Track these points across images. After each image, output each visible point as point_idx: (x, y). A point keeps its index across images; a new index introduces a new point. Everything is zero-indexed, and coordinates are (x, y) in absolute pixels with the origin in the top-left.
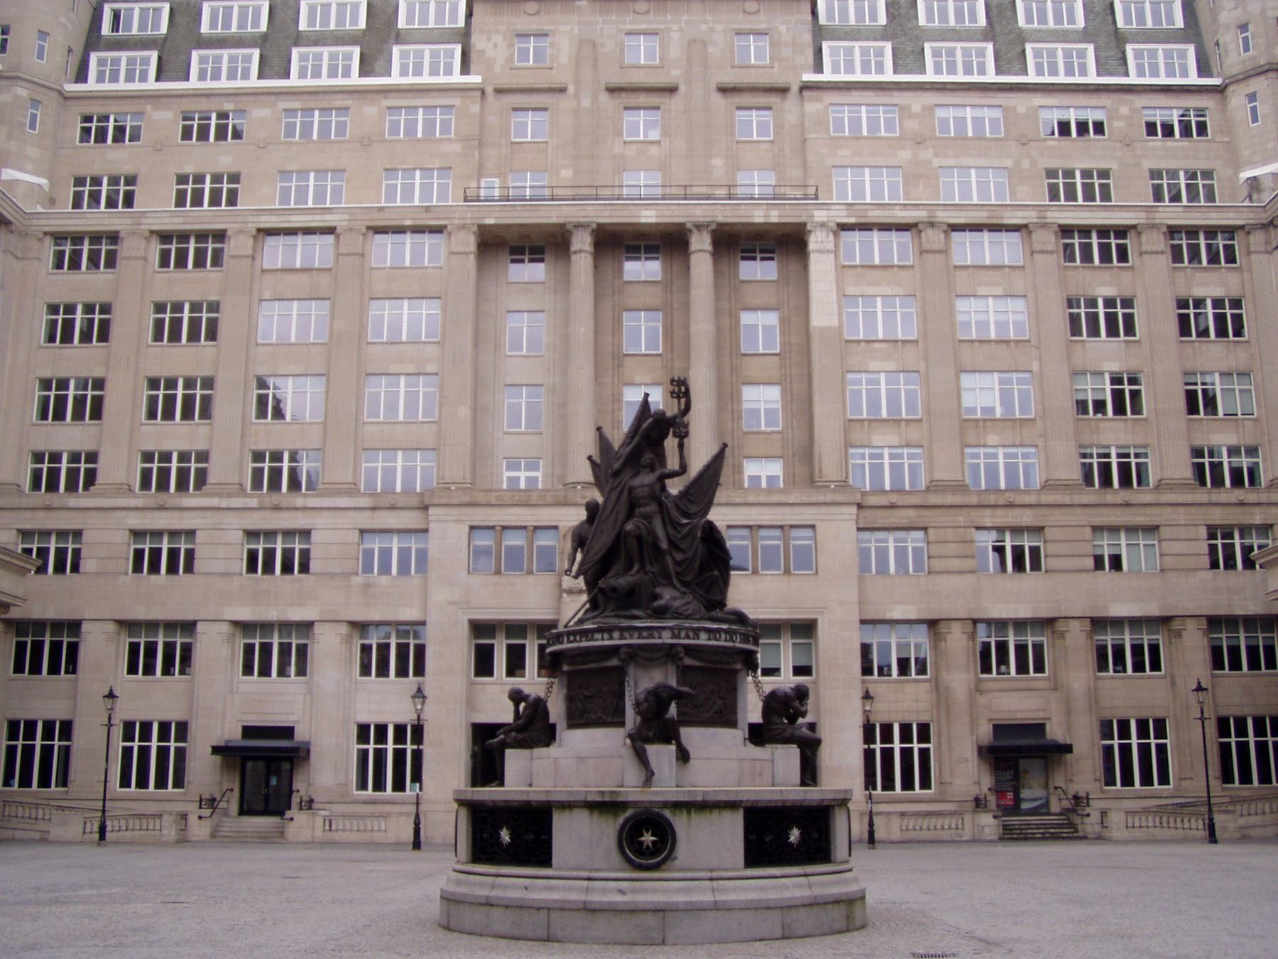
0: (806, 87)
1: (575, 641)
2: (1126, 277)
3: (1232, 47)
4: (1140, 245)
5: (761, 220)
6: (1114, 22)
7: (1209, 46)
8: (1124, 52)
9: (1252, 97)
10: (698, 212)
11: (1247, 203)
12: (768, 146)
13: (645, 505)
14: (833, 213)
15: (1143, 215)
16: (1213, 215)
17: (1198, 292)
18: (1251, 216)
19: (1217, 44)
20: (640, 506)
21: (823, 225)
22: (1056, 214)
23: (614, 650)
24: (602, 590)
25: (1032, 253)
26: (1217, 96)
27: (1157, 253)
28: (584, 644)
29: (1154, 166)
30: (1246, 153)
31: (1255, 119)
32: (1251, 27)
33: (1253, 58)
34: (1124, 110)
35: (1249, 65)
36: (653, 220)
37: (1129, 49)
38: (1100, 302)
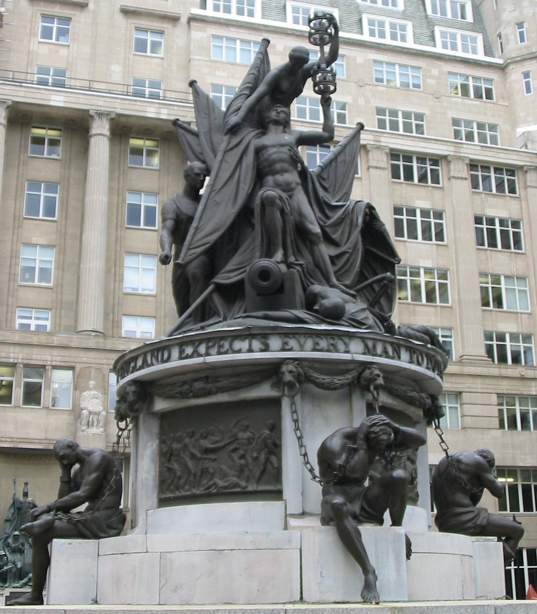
0: (192, 19)
2: (437, 194)
3: (511, 37)
4: (449, 171)
5: (153, 116)
6: (425, 10)
7: (493, 37)
8: (433, 32)
10: (100, 103)
11: (523, 150)
12: (159, 61)
13: (283, 171)
15: (452, 149)
16: (501, 155)
17: (490, 212)
18: (528, 159)
19: (500, 36)
22: (388, 140)
23: (271, 371)
24: (219, 288)
25: (368, 169)
27: (462, 178)
28: (215, 358)
29: (456, 116)
30: (522, 114)
32: (525, 25)
33: (527, 47)
34: (435, 72)
36: (61, 105)
37: (437, 30)
38: (418, 213)
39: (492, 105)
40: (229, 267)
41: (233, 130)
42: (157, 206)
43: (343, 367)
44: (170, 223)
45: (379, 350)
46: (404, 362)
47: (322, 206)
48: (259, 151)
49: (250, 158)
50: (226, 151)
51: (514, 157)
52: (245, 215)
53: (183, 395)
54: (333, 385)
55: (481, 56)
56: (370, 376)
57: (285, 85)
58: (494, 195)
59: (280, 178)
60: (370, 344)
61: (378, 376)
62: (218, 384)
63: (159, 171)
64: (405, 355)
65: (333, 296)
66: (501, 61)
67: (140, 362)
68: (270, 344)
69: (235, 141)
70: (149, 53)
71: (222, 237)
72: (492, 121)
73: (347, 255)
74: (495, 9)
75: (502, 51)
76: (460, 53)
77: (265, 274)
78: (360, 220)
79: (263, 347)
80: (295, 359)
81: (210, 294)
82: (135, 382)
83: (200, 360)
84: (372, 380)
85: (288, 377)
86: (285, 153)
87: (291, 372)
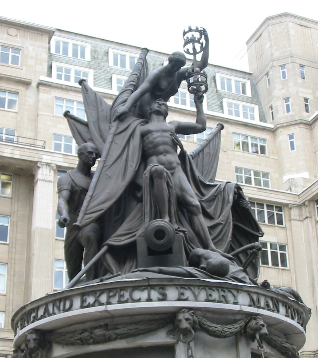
0: (41, 84)
1: (97, 303)
3: (280, 108)
6: (216, 86)
7: (266, 109)
8: (221, 102)
9: (291, 137)
11: (289, 192)
12: (14, 114)
13: (166, 152)
14: (54, 158)
16: (273, 195)
18: (292, 199)
19: (271, 108)
20: (158, 154)
21: (48, 164)
23: (168, 320)
24: (112, 250)
26: (271, 134)
28: (115, 307)
29: (238, 166)
31: (292, 148)
32: (291, 100)
33: (292, 116)
35: (290, 119)
37: (225, 101)
39: (265, 158)
40: (120, 231)
41: (121, 118)
42: (9, 225)
43: (231, 317)
44: (66, 193)
45: (262, 303)
46: (281, 316)
47: (199, 185)
48: (143, 135)
49: (136, 142)
50: (116, 135)
51: (282, 197)
52: (133, 190)
53: (84, 342)
54: (224, 333)
55: (257, 121)
56: (256, 326)
57: (164, 84)
58: (267, 225)
59: (162, 158)
60: (255, 297)
61: (263, 326)
62: (117, 331)
63: (11, 198)
64: (282, 309)
65: (216, 256)
66: (272, 126)
67: (41, 312)
68: (167, 294)
69: (123, 126)
70: (6, 109)
71: (110, 209)
72: (265, 170)
73: (221, 226)
74: (268, 87)
75: (273, 119)
76: (241, 119)
77: (160, 233)
78: (231, 198)
79: (160, 297)
80: (190, 309)
81: (104, 255)
82: (35, 331)
83: (102, 308)
84: (257, 330)
85: (185, 325)
86: (167, 137)
87: (187, 319)
